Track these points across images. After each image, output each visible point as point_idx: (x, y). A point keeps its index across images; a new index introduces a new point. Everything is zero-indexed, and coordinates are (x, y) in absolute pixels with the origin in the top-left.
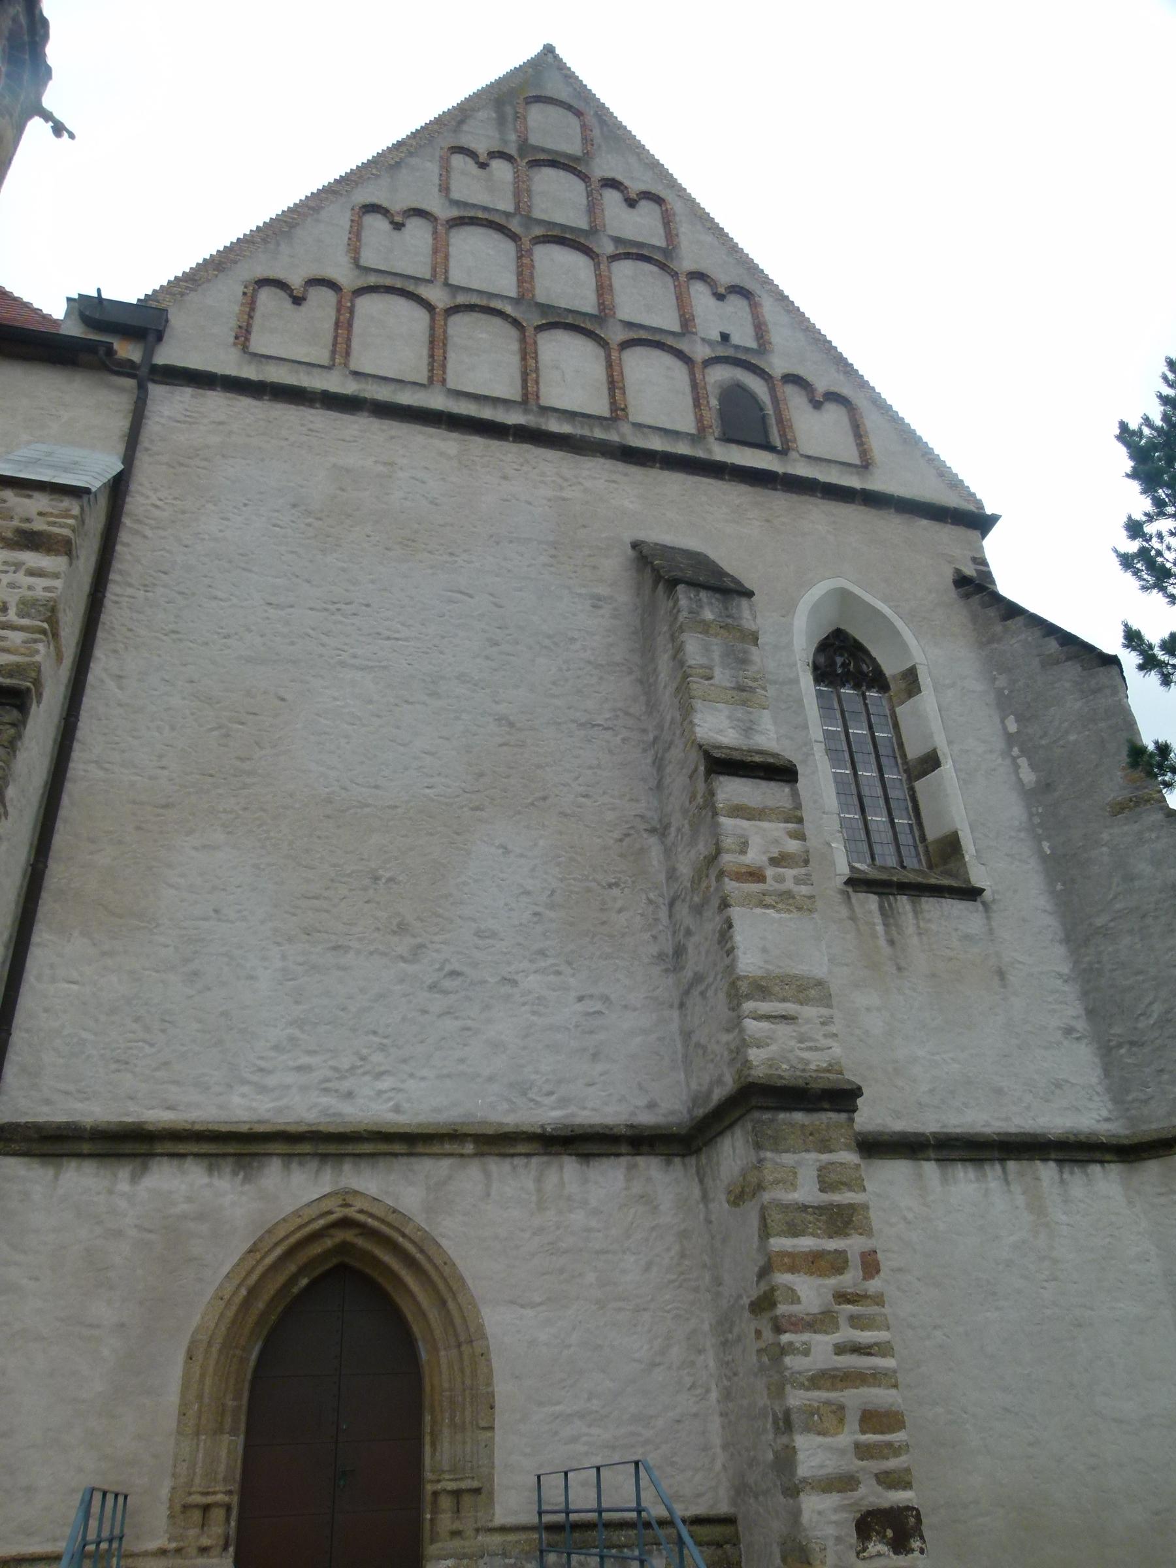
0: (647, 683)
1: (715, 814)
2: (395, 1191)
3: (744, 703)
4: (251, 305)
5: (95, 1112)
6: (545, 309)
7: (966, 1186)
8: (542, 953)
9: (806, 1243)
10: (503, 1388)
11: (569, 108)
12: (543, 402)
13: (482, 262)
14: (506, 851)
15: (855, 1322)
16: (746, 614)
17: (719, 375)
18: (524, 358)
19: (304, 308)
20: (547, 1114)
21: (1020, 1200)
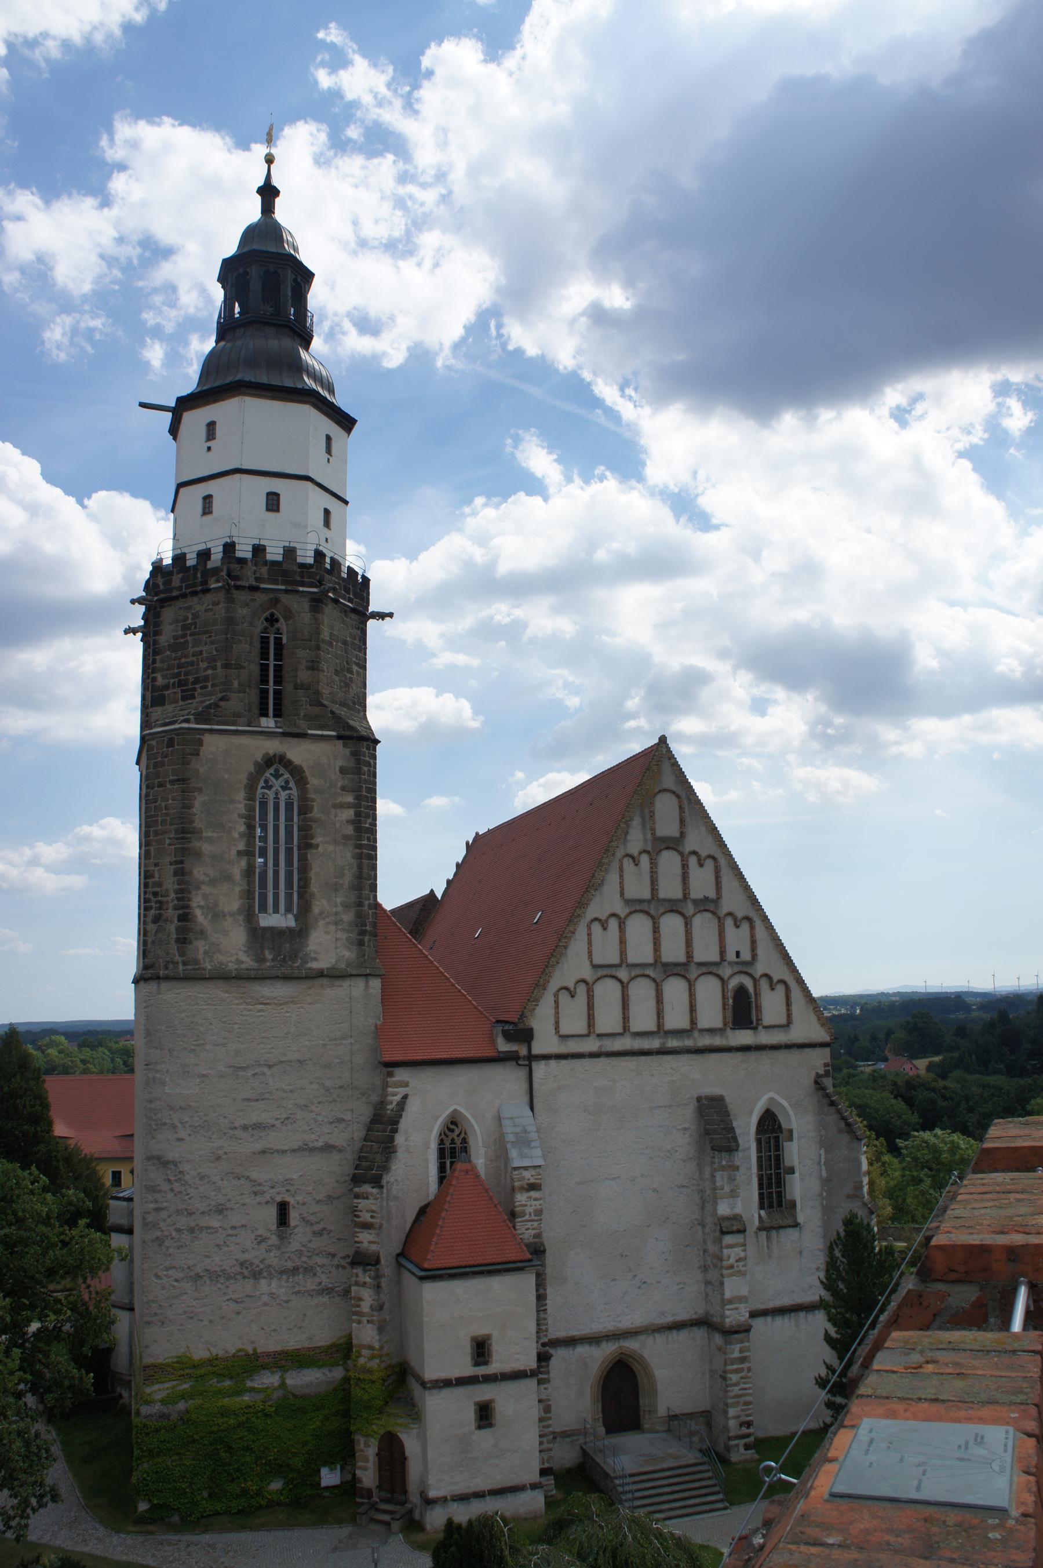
0: (701, 1172)
1: (722, 1248)
2: (632, 1345)
3: (733, 1197)
4: (556, 1002)
6: (666, 965)
7: (779, 1322)
8: (667, 1272)
9: (735, 1367)
10: (660, 1388)
11: (674, 793)
14: (657, 1239)
15: (744, 1383)
17: (733, 983)
20: (669, 1319)
21: (793, 1323)
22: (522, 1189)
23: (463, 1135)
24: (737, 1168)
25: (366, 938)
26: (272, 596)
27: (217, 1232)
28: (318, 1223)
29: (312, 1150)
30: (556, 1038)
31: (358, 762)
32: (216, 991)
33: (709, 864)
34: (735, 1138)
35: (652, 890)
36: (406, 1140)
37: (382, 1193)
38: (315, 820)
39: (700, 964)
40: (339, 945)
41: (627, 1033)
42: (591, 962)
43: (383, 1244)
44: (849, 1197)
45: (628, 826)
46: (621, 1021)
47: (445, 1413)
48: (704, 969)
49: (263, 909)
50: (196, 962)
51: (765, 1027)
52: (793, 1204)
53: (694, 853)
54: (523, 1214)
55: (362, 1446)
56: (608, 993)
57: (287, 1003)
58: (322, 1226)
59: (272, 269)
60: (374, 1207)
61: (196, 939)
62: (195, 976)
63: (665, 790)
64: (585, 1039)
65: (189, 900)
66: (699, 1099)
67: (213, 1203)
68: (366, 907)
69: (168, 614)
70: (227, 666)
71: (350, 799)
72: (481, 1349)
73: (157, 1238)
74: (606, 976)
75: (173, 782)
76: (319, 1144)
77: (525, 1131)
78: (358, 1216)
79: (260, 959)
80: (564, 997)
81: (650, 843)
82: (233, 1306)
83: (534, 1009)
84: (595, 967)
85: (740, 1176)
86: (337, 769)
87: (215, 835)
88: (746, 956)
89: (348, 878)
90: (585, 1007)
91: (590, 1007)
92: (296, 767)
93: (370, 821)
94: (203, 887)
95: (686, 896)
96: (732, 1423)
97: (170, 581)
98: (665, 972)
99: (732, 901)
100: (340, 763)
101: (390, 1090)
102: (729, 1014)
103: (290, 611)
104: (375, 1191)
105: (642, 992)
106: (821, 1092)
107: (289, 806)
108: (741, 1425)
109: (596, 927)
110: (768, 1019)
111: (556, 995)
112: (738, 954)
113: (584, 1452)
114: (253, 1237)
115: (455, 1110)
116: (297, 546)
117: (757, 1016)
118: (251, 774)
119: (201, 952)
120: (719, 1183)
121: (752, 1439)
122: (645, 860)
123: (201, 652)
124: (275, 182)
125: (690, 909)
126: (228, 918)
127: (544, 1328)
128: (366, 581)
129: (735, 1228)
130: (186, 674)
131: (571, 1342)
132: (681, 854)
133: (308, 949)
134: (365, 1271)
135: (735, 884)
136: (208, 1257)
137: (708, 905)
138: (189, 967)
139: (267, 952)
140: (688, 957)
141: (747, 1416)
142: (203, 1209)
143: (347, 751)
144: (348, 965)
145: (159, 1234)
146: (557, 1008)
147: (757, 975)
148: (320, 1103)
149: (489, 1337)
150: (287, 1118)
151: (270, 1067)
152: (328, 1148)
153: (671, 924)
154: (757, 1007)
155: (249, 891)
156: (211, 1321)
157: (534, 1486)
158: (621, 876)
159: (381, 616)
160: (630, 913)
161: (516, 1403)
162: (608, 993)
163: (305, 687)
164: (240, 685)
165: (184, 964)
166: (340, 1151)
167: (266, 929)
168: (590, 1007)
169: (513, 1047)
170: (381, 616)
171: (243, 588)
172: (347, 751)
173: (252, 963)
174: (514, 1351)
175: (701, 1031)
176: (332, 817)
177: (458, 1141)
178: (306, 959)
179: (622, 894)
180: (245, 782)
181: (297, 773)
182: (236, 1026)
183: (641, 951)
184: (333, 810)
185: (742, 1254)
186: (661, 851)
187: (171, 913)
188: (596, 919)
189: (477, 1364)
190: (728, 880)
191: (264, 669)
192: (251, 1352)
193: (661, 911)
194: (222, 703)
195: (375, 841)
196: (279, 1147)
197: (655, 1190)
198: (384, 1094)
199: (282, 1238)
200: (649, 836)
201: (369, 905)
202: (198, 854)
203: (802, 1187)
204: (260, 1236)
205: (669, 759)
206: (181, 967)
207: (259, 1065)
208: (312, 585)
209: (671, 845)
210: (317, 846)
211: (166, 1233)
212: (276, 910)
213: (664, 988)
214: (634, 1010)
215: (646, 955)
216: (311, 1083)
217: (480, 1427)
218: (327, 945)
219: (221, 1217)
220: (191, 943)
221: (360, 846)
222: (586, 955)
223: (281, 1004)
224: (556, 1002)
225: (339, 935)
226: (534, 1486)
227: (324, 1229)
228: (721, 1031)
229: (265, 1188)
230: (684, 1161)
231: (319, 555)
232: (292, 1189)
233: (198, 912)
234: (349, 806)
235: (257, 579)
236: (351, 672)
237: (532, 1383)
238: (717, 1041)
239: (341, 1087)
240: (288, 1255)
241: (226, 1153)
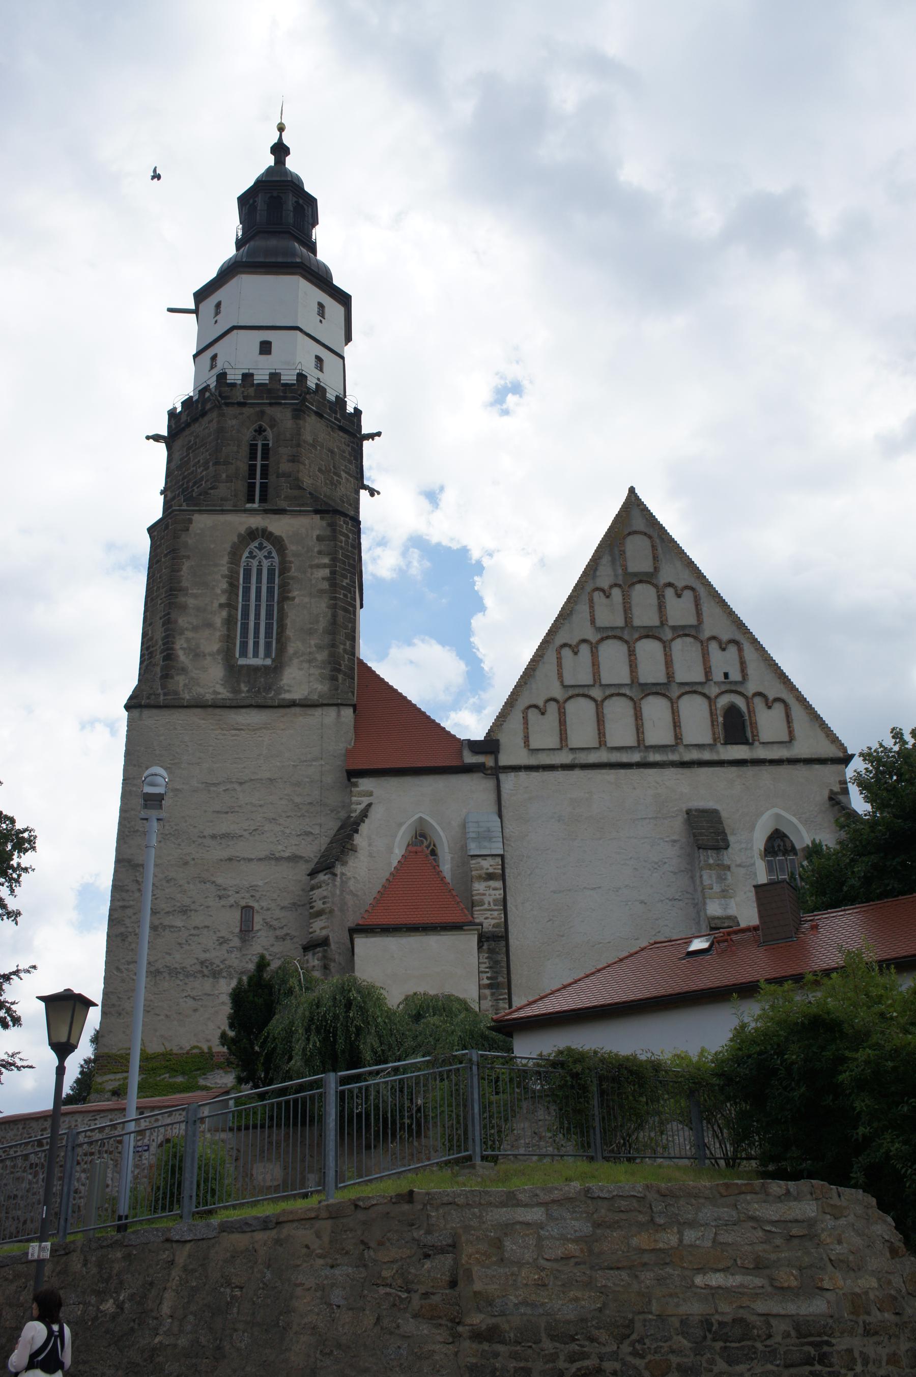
3: (724, 897)
11: (645, 534)
12: (647, 744)
13: (614, 663)
16: (726, 858)
17: (723, 701)
18: (636, 720)
19: (546, 716)
22: (480, 878)
23: (432, 847)
24: (728, 868)
25: (340, 677)
26: (258, 409)
27: (180, 931)
28: (282, 928)
29: (278, 859)
31: (334, 531)
32: (194, 717)
33: (688, 594)
36: (370, 845)
37: (334, 880)
38: (293, 578)
40: (312, 679)
41: (603, 747)
42: (562, 682)
46: (597, 736)
49: (244, 654)
50: (176, 693)
51: (761, 743)
53: (670, 585)
54: (482, 903)
56: (581, 713)
57: (261, 728)
58: (284, 931)
59: (275, 194)
61: (178, 674)
62: (175, 705)
63: (635, 532)
64: (556, 752)
65: (173, 643)
66: (688, 812)
67: (179, 904)
68: (341, 651)
69: (179, 443)
70: (216, 463)
71: (326, 560)
73: (121, 934)
74: (578, 695)
75: (166, 555)
76: (287, 854)
79: (236, 691)
80: (533, 715)
81: (620, 577)
82: (191, 1002)
83: (501, 725)
84: (565, 687)
86: (315, 537)
87: (200, 591)
88: (735, 676)
89: (322, 624)
90: (557, 724)
91: (562, 723)
92: (276, 537)
94: (186, 632)
95: (663, 623)
97: (180, 419)
98: (643, 691)
99: (713, 625)
100: (317, 532)
101: (354, 799)
102: (720, 730)
103: (275, 420)
105: (619, 714)
106: (836, 807)
107: (271, 572)
109: (566, 652)
110: (765, 736)
112: (726, 675)
114: (215, 938)
115: (421, 819)
116: (282, 372)
117: (752, 732)
118: (234, 543)
119: (181, 685)
120: (707, 881)
122: (616, 593)
123: (199, 461)
124: (286, 142)
125: (668, 635)
126: (207, 657)
128: (358, 412)
130: (187, 482)
132: (655, 586)
133: (282, 683)
134: (314, 954)
135: (718, 610)
136: (170, 954)
138: (169, 697)
139: (242, 685)
140: (668, 678)
142: (167, 910)
143: (324, 523)
144: (320, 696)
145: (123, 930)
147: (750, 694)
148: (288, 817)
150: (255, 830)
151: (241, 784)
152: (295, 859)
154: (751, 724)
155: (228, 636)
156: (167, 1016)
159: (372, 436)
163: (287, 475)
164: (227, 476)
165: (165, 694)
167: (242, 666)
168: (562, 723)
169: (480, 759)
170: (372, 436)
171: (233, 404)
172: (324, 523)
173: (228, 694)
176: (309, 575)
178: (280, 690)
179: (593, 621)
180: (229, 549)
181: (277, 542)
182: (211, 748)
184: (309, 570)
186: (633, 584)
187: (159, 657)
190: (707, 607)
191: (252, 468)
192: (206, 1050)
193: (636, 636)
194: (212, 491)
196: (246, 856)
197: (642, 902)
199: (244, 941)
200: (620, 571)
201: (345, 650)
202: (183, 608)
204: (222, 937)
205: (638, 505)
206: (162, 697)
207: (232, 782)
208: (293, 398)
209: (645, 579)
210: (294, 598)
211: (130, 930)
212: (256, 655)
213: (642, 706)
214: (609, 727)
215: (622, 676)
216: (281, 799)
218: (299, 680)
219: (185, 917)
220: (172, 678)
221: (335, 598)
222: (556, 676)
223: (254, 730)
225: (312, 671)
227: (287, 934)
229: (230, 893)
230: (675, 873)
231: (302, 377)
232: (258, 895)
233: (180, 653)
234: (325, 566)
235: (244, 397)
236: (340, 476)
238: (707, 756)
239: (311, 803)
240: (249, 957)
241: (193, 859)
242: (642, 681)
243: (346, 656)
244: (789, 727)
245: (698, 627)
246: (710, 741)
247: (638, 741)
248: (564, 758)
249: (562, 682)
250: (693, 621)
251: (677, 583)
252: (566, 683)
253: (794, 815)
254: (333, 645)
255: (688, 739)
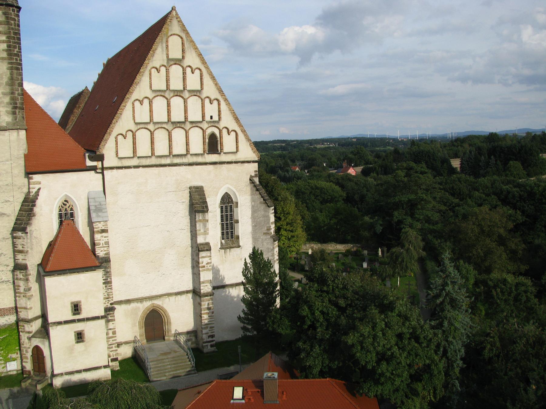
2: (157, 302)
4: (116, 141)
5: (123, 298)
6: (173, 123)
11: (179, 36)
17: (209, 131)
20: (176, 290)
22: (99, 232)
23: (71, 207)
25: (17, 111)
30: (117, 158)
31: (7, 18)
34: (207, 207)
35: (167, 85)
37: (27, 236)
39: (192, 122)
42: (134, 121)
43: (33, 260)
44: (264, 234)
45: (154, 53)
47: (61, 336)
48: (212, 124)
51: (225, 153)
52: (238, 237)
53: (190, 66)
54: (99, 244)
55: (25, 352)
56: (143, 136)
60: (23, 243)
63: (174, 34)
64: (131, 159)
66: (190, 188)
68: (16, 95)
72: (76, 308)
77: (100, 205)
78: (16, 247)
81: (166, 61)
85: (210, 225)
88: (216, 118)
91: (134, 143)
93: (17, 50)
95: (184, 88)
96: (205, 336)
104: (23, 235)
105: (161, 136)
106: (253, 184)
108: (209, 337)
109: (137, 104)
110: (225, 150)
111: (116, 138)
112: (211, 117)
113: (135, 350)
121: (214, 342)
122: (163, 70)
127: (111, 296)
129: (206, 249)
131: (128, 302)
132: (183, 67)
134: (20, 273)
137: (196, 93)
140: (185, 119)
141: (212, 332)
146: (117, 144)
149: (80, 302)
153: (176, 102)
157: (105, 367)
158: (150, 78)
160: (155, 97)
161: (95, 331)
162: (143, 136)
166: (8, 216)
168: (134, 143)
174: (93, 306)
175: (191, 155)
177: (69, 210)
179: (151, 87)
183: (160, 115)
185: (209, 261)
186: (171, 65)
188: (137, 100)
189: (74, 314)
195: (21, 60)
198: (29, 188)
201: (19, 94)
203: (244, 228)
209: (178, 63)
217: (77, 342)
224: (116, 141)
226: (105, 367)
228: (202, 155)
234: (3, 42)
237: (103, 321)
238: (200, 159)
242: (173, 120)
243: (19, 97)
244: (237, 145)
245: (200, 91)
246: (202, 152)
247: (170, 152)
248: (135, 162)
249: (134, 121)
250: (199, 88)
251: (192, 66)
252: (137, 121)
253: (235, 188)
254: (12, 93)
255: (192, 151)
